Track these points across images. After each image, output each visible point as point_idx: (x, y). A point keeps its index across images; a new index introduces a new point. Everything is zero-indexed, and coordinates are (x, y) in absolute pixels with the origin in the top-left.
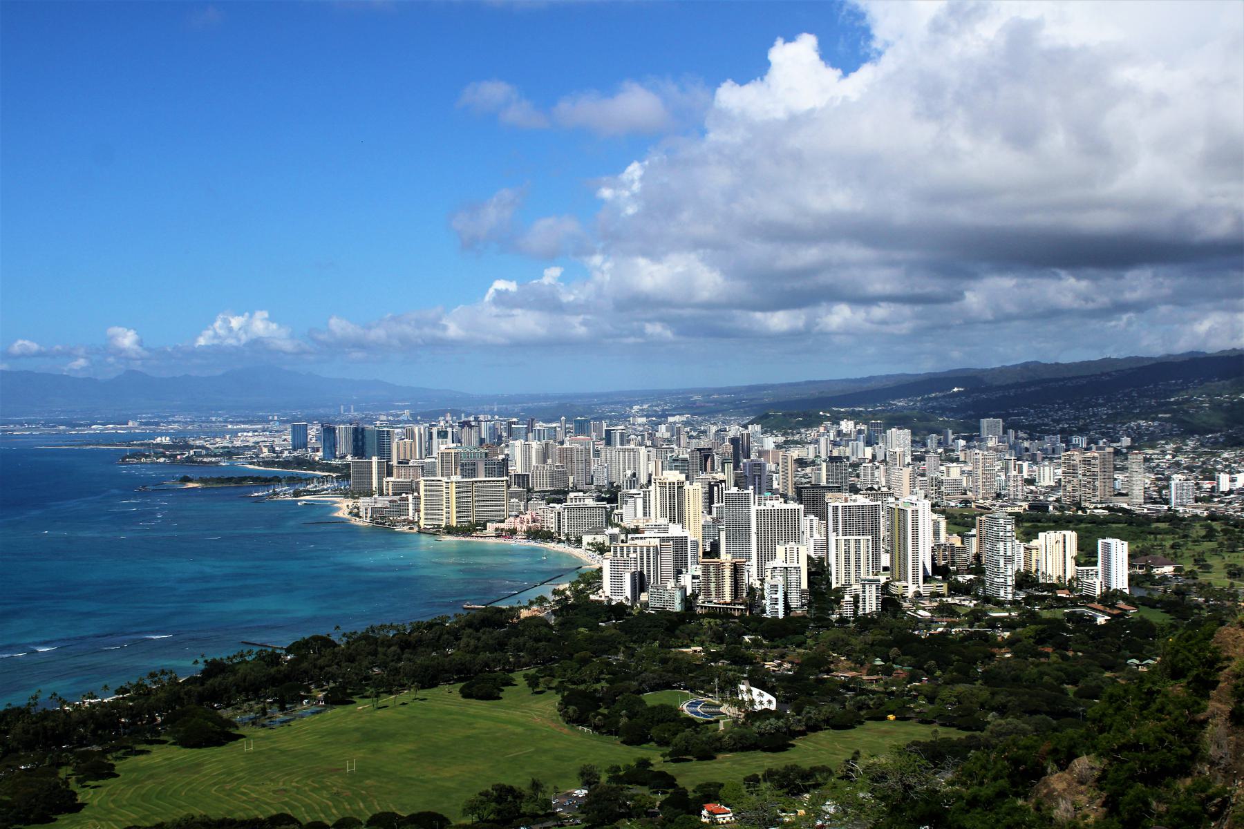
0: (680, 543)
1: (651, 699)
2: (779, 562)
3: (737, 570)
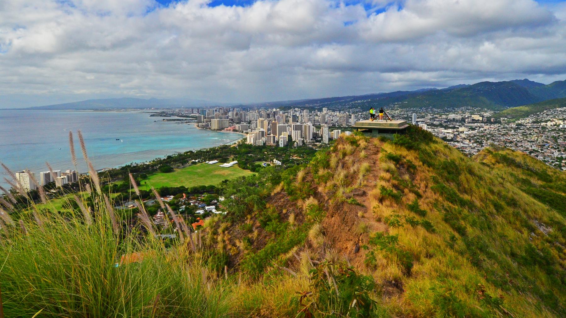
0: (263, 132)
1: (257, 163)
2: (282, 136)
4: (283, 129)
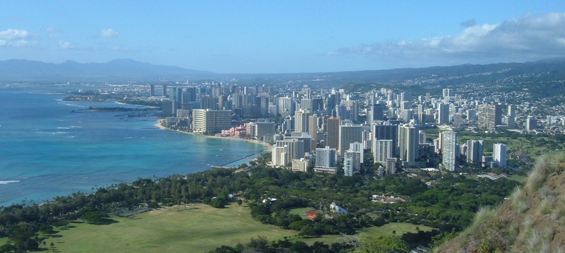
0: (307, 141)
2: (350, 151)
3: (332, 154)
4: (353, 136)
